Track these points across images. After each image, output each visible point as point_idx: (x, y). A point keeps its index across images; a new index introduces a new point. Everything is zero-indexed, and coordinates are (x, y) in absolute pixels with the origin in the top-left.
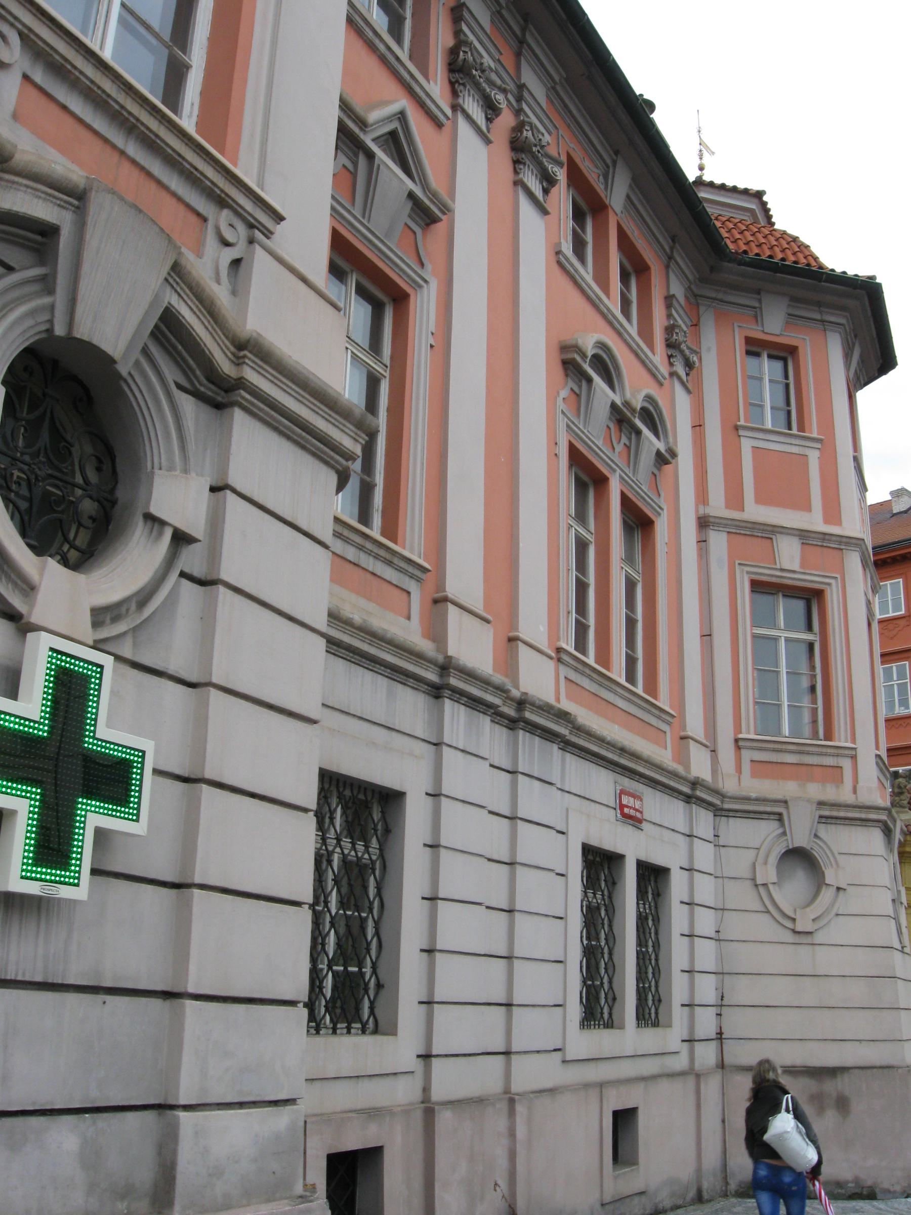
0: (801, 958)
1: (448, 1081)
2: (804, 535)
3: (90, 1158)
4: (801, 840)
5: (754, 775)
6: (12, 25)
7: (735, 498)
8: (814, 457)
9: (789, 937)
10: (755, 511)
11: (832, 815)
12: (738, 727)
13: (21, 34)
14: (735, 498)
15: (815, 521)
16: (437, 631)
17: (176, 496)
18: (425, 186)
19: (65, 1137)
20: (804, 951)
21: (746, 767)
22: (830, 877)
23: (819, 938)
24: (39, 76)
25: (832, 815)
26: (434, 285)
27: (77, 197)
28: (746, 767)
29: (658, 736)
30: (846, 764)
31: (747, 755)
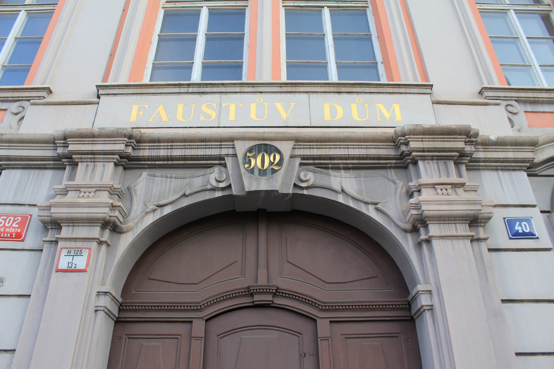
6: (512, 100)
13: (516, 101)
24: (529, 108)
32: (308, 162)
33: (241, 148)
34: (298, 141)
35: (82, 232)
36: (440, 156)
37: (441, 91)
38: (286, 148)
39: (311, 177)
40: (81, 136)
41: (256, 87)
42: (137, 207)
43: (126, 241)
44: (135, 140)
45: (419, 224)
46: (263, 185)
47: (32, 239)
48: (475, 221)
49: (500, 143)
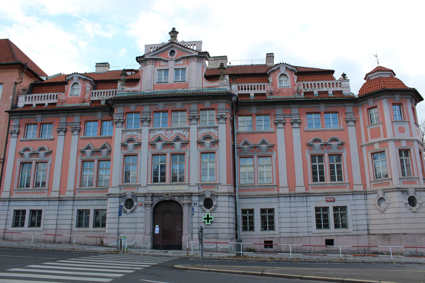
0: (383, 216)
1: (283, 235)
2: (379, 142)
3: (214, 236)
4: (381, 196)
5: (374, 187)
7: (367, 140)
8: (381, 126)
9: (380, 213)
10: (371, 141)
11: (385, 191)
12: (370, 180)
14: (367, 140)
15: (382, 139)
16: (278, 191)
17: (215, 203)
18: (269, 144)
19: (213, 235)
20: (383, 215)
21: (372, 185)
22: (387, 202)
23: (385, 212)
25: (385, 191)
26: (275, 152)
27: (204, 192)
28: (372, 185)
29: (346, 187)
30: (390, 181)
31: (372, 184)
32: (172, 196)
33: (165, 194)
34: (171, 193)
35: (149, 205)
36: (187, 196)
37: (192, 183)
38: (170, 194)
39: (172, 198)
40: (147, 194)
41: (167, 185)
42: (154, 202)
43: (153, 206)
44: (153, 194)
45: (183, 204)
46: (167, 199)
47: (143, 205)
48: (189, 204)
49: (195, 193)
